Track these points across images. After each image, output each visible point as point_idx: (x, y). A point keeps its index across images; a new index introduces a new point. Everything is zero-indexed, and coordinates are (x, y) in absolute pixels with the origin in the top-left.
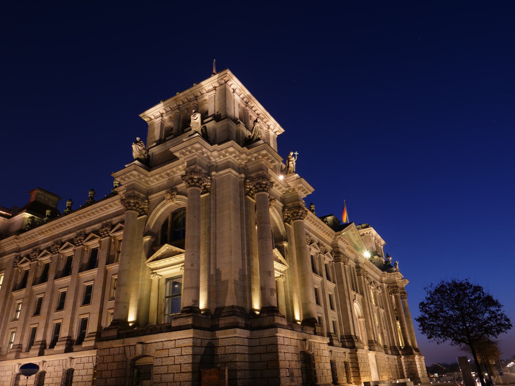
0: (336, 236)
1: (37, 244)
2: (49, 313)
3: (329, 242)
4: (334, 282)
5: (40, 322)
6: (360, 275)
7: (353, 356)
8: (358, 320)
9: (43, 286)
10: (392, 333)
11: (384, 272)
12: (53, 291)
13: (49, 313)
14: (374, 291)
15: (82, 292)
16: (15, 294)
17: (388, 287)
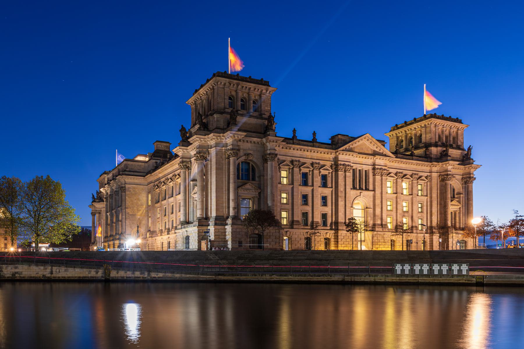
0: (336, 153)
1: (159, 179)
2: (169, 215)
3: (329, 158)
4: (332, 187)
5: (166, 218)
6: (375, 175)
7: (336, 235)
8: (365, 210)
9: (172, 199)
10: (431, 216)
11: (432, 163)
12: (169, 204)
13: (169, 215)
14: (410, 183)
15: (178, 205)
16: (156, 205)
17: (440, 175)
